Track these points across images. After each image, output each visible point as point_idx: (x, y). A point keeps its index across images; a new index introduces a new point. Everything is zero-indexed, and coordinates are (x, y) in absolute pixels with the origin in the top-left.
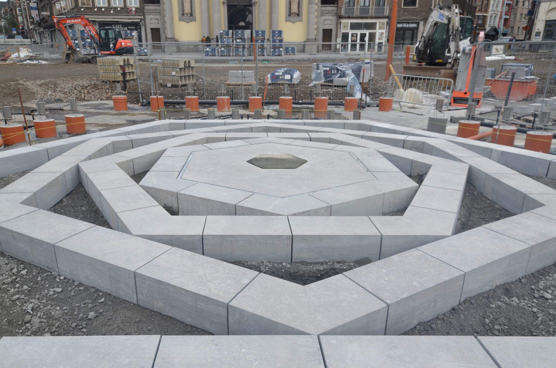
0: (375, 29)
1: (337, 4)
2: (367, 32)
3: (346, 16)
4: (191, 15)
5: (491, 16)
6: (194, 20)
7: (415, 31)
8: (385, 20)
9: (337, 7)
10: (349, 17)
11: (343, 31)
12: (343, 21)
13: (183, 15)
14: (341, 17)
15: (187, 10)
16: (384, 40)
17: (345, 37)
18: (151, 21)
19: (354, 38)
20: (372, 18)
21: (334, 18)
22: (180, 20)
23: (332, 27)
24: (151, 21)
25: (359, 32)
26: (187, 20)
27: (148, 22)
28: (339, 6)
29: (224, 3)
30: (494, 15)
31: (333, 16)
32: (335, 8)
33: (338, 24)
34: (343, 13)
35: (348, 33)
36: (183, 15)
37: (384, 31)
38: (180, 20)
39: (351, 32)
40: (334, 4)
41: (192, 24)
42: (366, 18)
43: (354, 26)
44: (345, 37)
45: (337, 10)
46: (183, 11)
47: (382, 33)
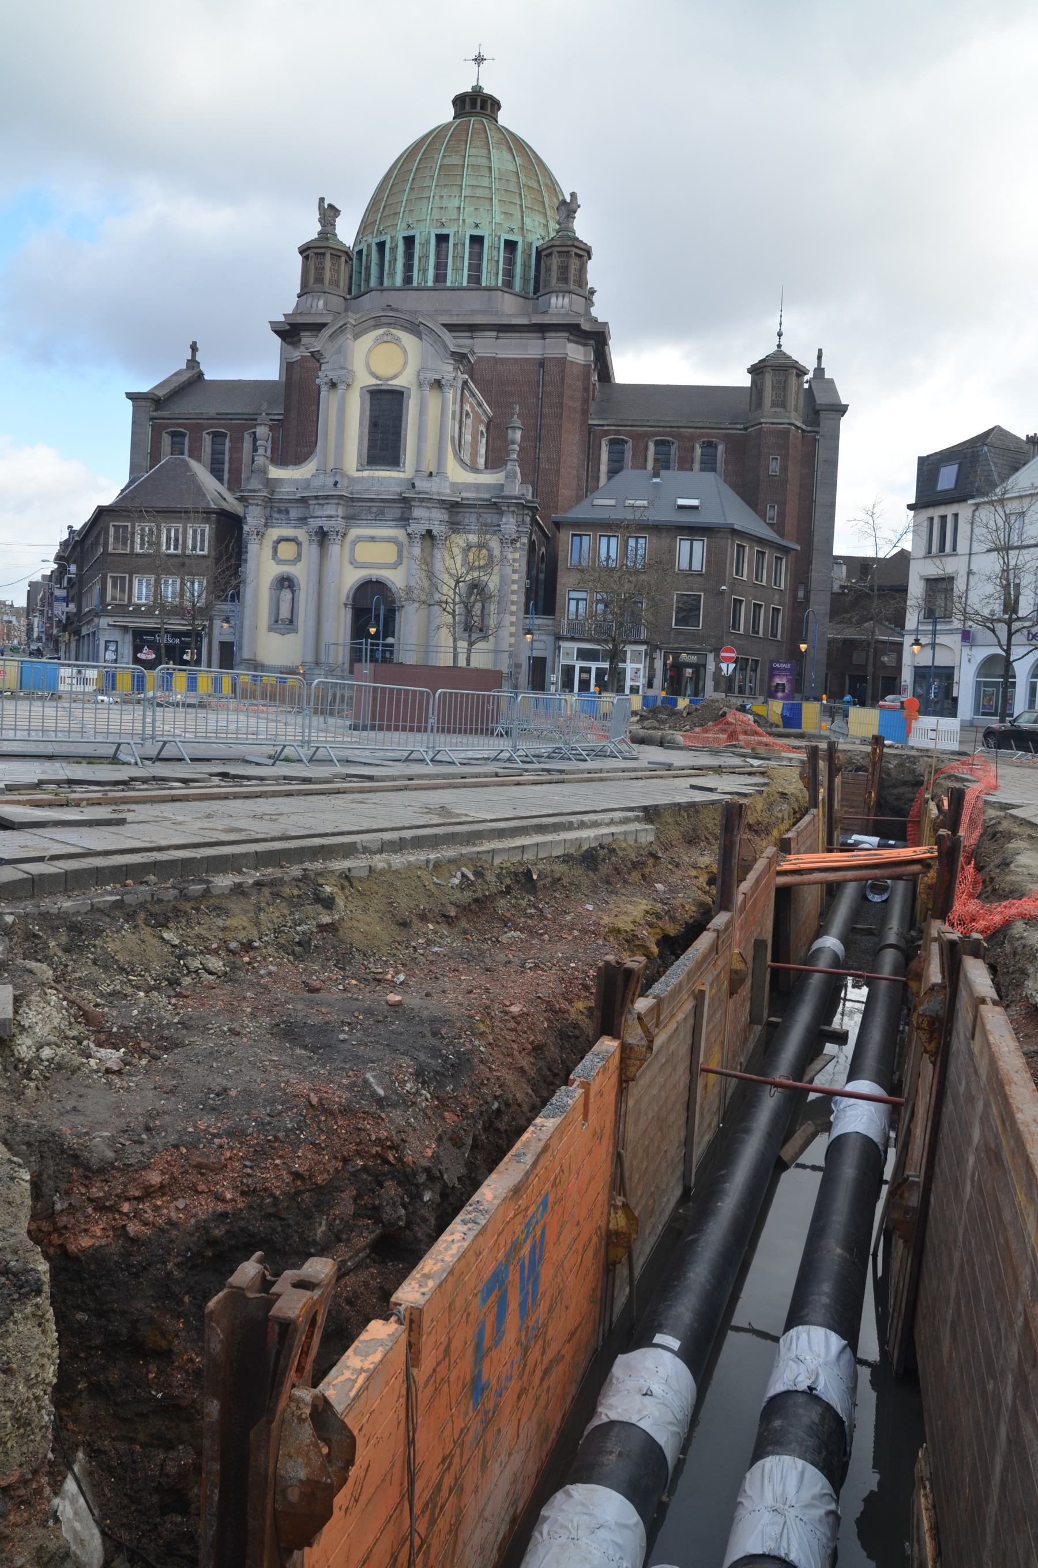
4: (291, 621)
6: (295, 631)
7: (702, 669)
8: (645, 647)
10: (573, 639)
11: (564, 661)
12: (564, 644)
13: (277, 621)
14: (559, 638)
15: (285, 613)
17: (569, 671)
18: (222, 631)
19: (585, 676)
21: (550, 639)
22: (270, 629)
23: (547, 654)
24: (222, 631)
25: (594, 666)
26: (282, 631)
27: (216, 631)
28: (557, 619)
29: (346, 605)
34: (564, 633)
36: (277, 621)
37: (641, 666)
38: (270, 629)
39: (578, 665)
41: (291, 637)
43: (583, 655)
44: (568, 671)
46: (278, 614)
47: (638, 670)
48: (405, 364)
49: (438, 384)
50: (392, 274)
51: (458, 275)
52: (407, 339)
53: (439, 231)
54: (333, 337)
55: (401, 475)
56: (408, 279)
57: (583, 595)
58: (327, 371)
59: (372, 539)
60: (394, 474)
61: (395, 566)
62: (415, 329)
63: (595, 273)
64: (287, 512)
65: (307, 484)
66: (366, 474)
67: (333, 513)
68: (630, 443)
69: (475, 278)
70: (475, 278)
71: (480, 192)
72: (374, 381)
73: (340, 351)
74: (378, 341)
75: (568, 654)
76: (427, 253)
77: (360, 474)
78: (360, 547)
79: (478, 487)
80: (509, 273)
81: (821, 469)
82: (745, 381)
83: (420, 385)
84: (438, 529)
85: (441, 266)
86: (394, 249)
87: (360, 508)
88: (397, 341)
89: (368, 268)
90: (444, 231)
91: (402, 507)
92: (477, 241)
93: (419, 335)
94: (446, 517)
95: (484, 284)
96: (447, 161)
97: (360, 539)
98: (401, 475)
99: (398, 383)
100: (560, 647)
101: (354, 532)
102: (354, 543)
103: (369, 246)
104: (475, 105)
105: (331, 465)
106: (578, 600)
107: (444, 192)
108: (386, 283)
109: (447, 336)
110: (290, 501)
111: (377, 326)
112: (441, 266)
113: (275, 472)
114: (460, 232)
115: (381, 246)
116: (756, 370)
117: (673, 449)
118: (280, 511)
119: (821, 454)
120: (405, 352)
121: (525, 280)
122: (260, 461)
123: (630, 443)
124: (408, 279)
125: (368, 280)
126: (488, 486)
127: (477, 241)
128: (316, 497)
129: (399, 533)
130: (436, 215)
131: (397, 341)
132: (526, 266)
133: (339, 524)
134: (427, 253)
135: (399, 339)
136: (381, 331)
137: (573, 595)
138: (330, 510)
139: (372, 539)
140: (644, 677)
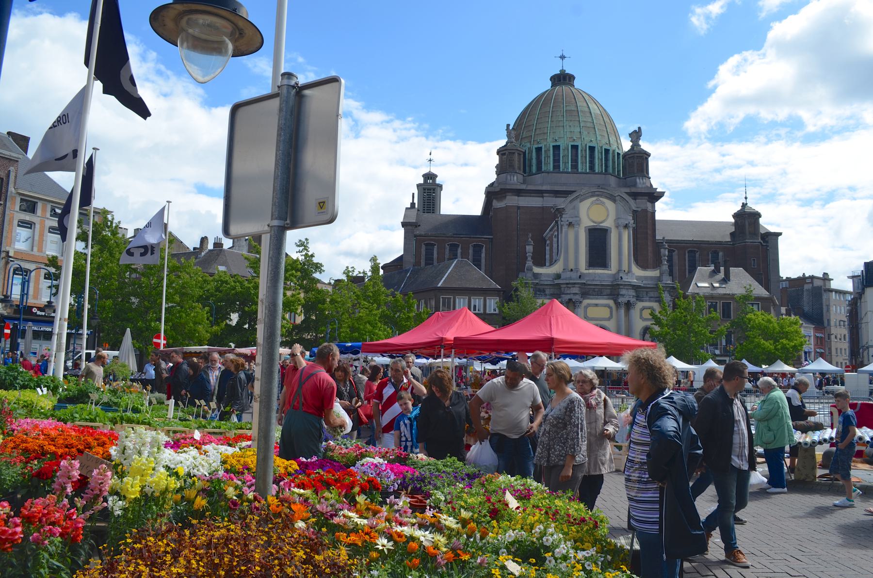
48: (608, 215)
49: (626, 226)
50: (547, 164)
51: (566, 164)
52: (609, 204)
53: (555, 144)
54: (571, 201)
55: (609, 272)
56: (556, 166)
58: (566, 218)
59: (596, 305)
60: (606, 272)
61: (609, 319)
62: (612, 198)
63: (654, 167)
64: (544, 291)
65: (558, 276)
66: (591, 271)
67: (577, 292)
68: (676, 252)
69: (592, 168)
70: (592, 168)
71: (589, 125)
72: (593, 224)
73: (574, 208)
74: (592, 203)
76: (566, 156)
77: (587, 271)
78: (589, 309)
79: (646, 278)
80: (606, 166)
82: (733, 220)
83: (617, 227)
84: (633, 300)
85: (575, 161)
86: (547, 151)
87: (589, 290)
88: (603, 204)
89: (530, 160)
90: (576, 144)
91: (613, 290)
92: (592, 149)
93: (614, 201)
94: (634, 294)
95: (580, 170)
96: (568, 108)
97: (589, 305)
98: (609, 272)
99: (604, 225)
101: (586, 302)
102: (586, 307)
103: (529, 149)
104: (562, 79)
105: (571, 266)
107: (571, 124)
108: (543, 169)
109: (631, 202)
110: (547, 285)
111: (592, 196)
112: (575, 161)
113: (537, 270)
114: (565, 143)
115: (539, 150)
116: (735, 216)
117: (697, 255)
118: (540, 290)
120: (607, 210)
121: (614, 169)
122: (529, 263)
123: (676, 252)
124: (556, 166)
125: (530, 166)
126: (651, 278)
127: (592, 149)
128: (567, 284)
129: (611, 302)
130: (569, 135)
131: (603, 204)
132: (614, 162)
133: (578, 297)
134: (566, 156)
135: (604, 203)
136: (594, 199)
138: (576, 290)
139: (596, 305)
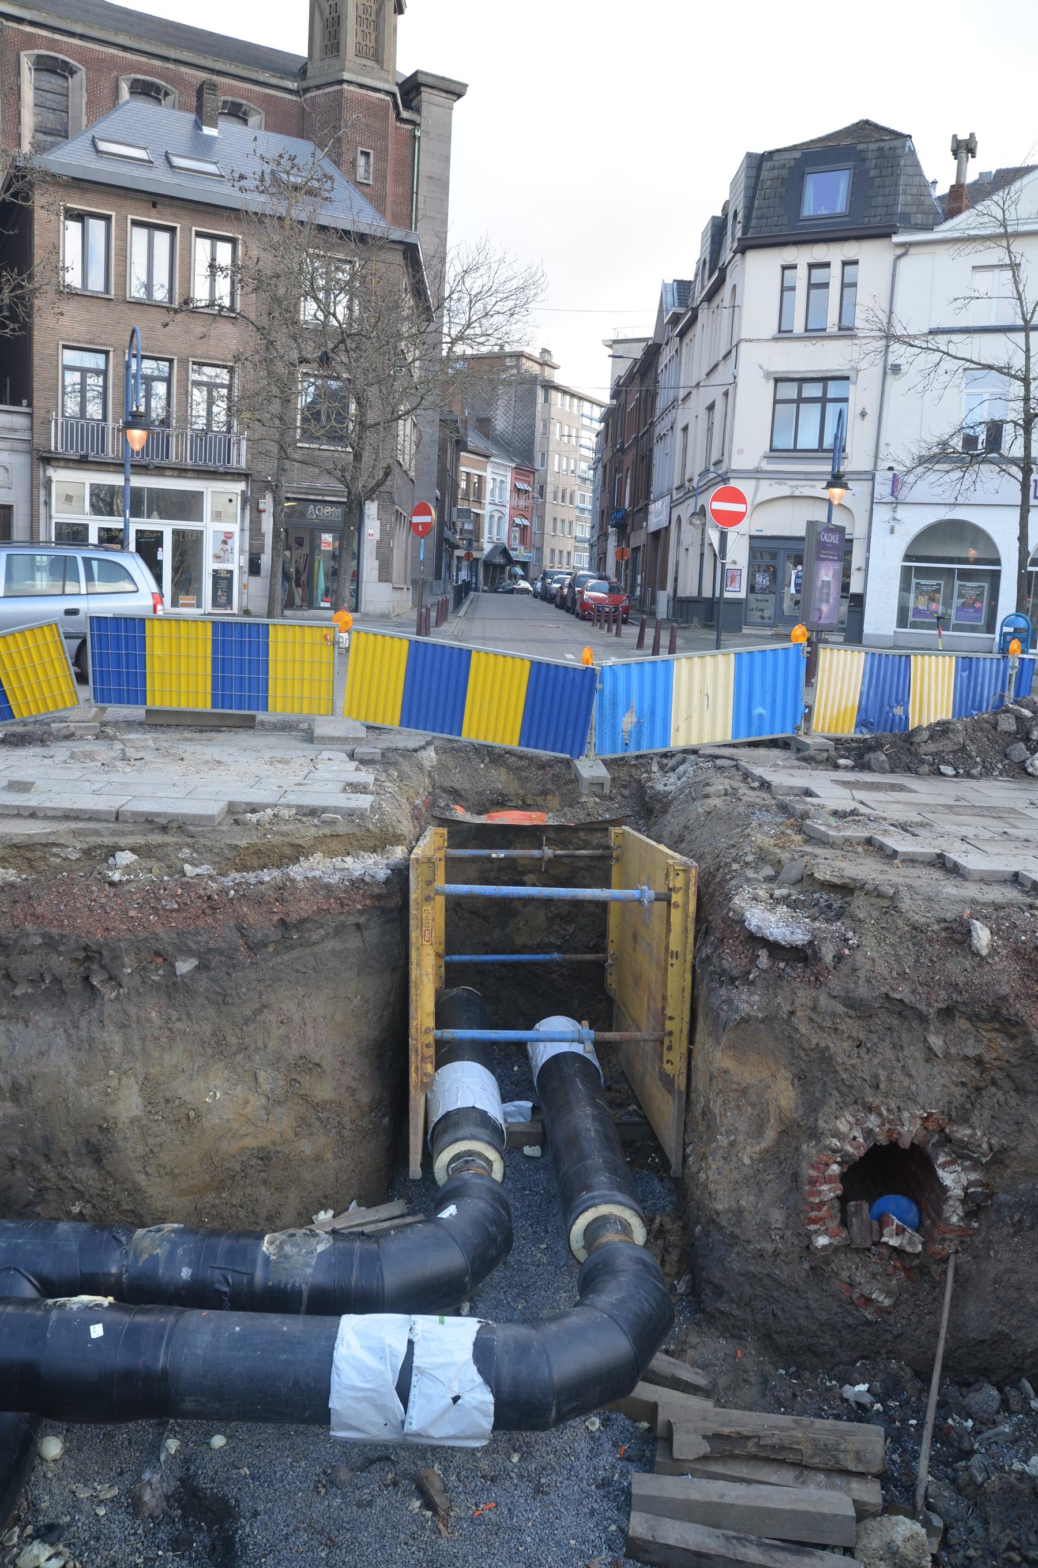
0: (200, 518)
1: (30, 405)
2: (167, 527)
3: (72, 454)
5: (492, 517)
8: (240, 486)
9: (30, 415)
10: (83, 462)
11: (62, 514)
12: (59, 476)
14: (47, 459)
16: (237, 563)
20: (182, 472)
21: (19, 462)
28: (39, 412)
30: (497, 515)
31: (13, 451)
32: (21, 422)
33: (38, 489)
34: (55, 443)
35: (86, 527)
37: (235, 528)
40: (20, 404)
42: (160, 471)
45: (31, 429)
47: (229, 536)
57: (96, 361)
75: (69, 498)
81: (424, 190)
100: (49, 482)
106: (84, 371)
119: (425, 165)
137: (70, 357)
140: (241, 551)
